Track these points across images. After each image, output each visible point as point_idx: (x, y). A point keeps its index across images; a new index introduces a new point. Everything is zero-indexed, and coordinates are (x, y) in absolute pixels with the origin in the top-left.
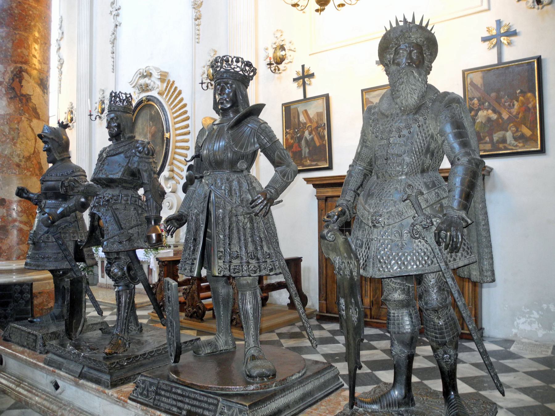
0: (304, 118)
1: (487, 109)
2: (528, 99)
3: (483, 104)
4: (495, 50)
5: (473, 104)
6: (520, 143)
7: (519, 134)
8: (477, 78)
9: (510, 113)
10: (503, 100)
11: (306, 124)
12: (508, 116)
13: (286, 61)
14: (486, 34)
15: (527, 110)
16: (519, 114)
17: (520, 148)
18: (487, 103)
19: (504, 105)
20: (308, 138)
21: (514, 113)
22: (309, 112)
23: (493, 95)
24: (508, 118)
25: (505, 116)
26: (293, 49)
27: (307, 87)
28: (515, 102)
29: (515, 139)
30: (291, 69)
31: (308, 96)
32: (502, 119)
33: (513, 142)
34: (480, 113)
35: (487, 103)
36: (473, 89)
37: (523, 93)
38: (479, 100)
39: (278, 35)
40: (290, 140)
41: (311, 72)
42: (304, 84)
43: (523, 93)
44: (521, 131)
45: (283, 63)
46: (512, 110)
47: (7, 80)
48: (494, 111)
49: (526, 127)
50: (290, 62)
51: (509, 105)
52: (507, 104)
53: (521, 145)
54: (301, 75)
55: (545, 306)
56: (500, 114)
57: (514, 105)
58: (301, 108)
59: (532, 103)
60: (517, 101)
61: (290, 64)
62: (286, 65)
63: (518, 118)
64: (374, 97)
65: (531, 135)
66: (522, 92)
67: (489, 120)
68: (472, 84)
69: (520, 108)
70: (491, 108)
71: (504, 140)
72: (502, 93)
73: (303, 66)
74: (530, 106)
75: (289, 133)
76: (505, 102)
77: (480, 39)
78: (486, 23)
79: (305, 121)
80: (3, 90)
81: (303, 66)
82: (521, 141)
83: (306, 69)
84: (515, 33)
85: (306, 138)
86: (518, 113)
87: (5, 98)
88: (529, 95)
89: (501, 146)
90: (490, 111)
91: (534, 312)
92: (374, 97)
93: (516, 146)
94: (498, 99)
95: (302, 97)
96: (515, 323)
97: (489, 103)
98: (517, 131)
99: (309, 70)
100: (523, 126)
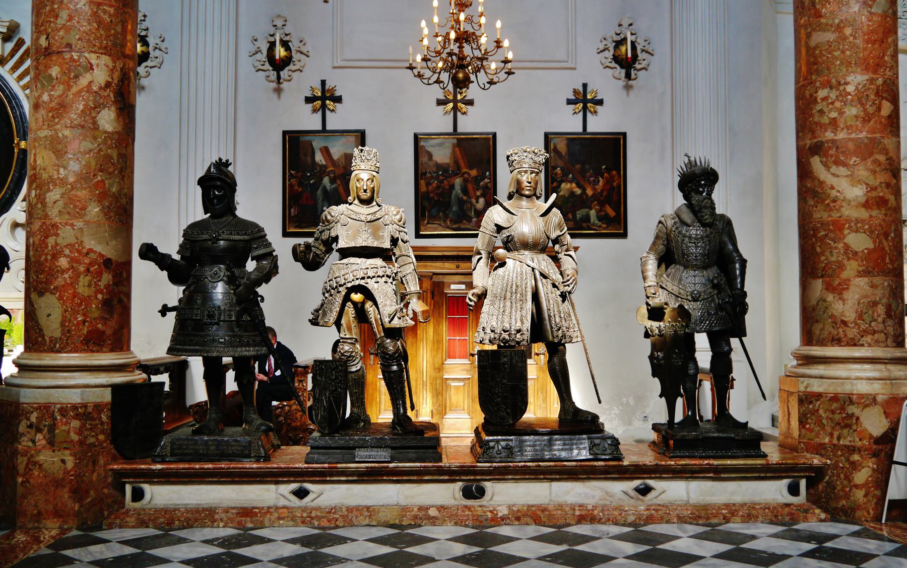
1: (571, 182)
2: (613, 177)
3: (567, 175)
5: (556, 174)
7: (603, 213)
8: (562, 146)
9: (595, 189)
11: (325, 167)
13: (291, 67)
17: (604, 229)
19: (589, 180)
20: (328, 188)
22: (332, 151)
23: (578, 166)
25: (590, 192)
26: (305, 51)
27: (328, 113)
29: (600, 219)
30: (303, 80)
31: (328, 128)
32: (587, 195)
33: (597, 222)
34: (563, 185)
37: (608, 170)
38: (562, 169)
39: (279, 23)
40: (296, 187)
41: (337, 94)
42: (324, 107)
43: (608, 170)
45: (287, 69)
47: (116, 81)
48: (579, 186)
51: (594, 181)
52: (592, 179)
53: (604, 226)
54: (320, 94)
55: (624, 400)
56: (584, 190)
57: (599, 181)
64: (433, 146)
67: (572, 193)
69: (604, 185)
71: (587, 218)
72: (587, 166)
73: (323, 83)
75: (295, 177)
77: (565, 102)
78: (569, 84)
79: (324, 163)
80: (112, 95)
81: (323, 83)
84: (600, 102)
85: (325, 187)
86: (602, 191)
87: (113, 108)
88: (614, 172)
89: (584, 225)
90: (574, 185)
92: (433, 146)
93: (600, 226)
94: (583, 172)
95: (319, 127)
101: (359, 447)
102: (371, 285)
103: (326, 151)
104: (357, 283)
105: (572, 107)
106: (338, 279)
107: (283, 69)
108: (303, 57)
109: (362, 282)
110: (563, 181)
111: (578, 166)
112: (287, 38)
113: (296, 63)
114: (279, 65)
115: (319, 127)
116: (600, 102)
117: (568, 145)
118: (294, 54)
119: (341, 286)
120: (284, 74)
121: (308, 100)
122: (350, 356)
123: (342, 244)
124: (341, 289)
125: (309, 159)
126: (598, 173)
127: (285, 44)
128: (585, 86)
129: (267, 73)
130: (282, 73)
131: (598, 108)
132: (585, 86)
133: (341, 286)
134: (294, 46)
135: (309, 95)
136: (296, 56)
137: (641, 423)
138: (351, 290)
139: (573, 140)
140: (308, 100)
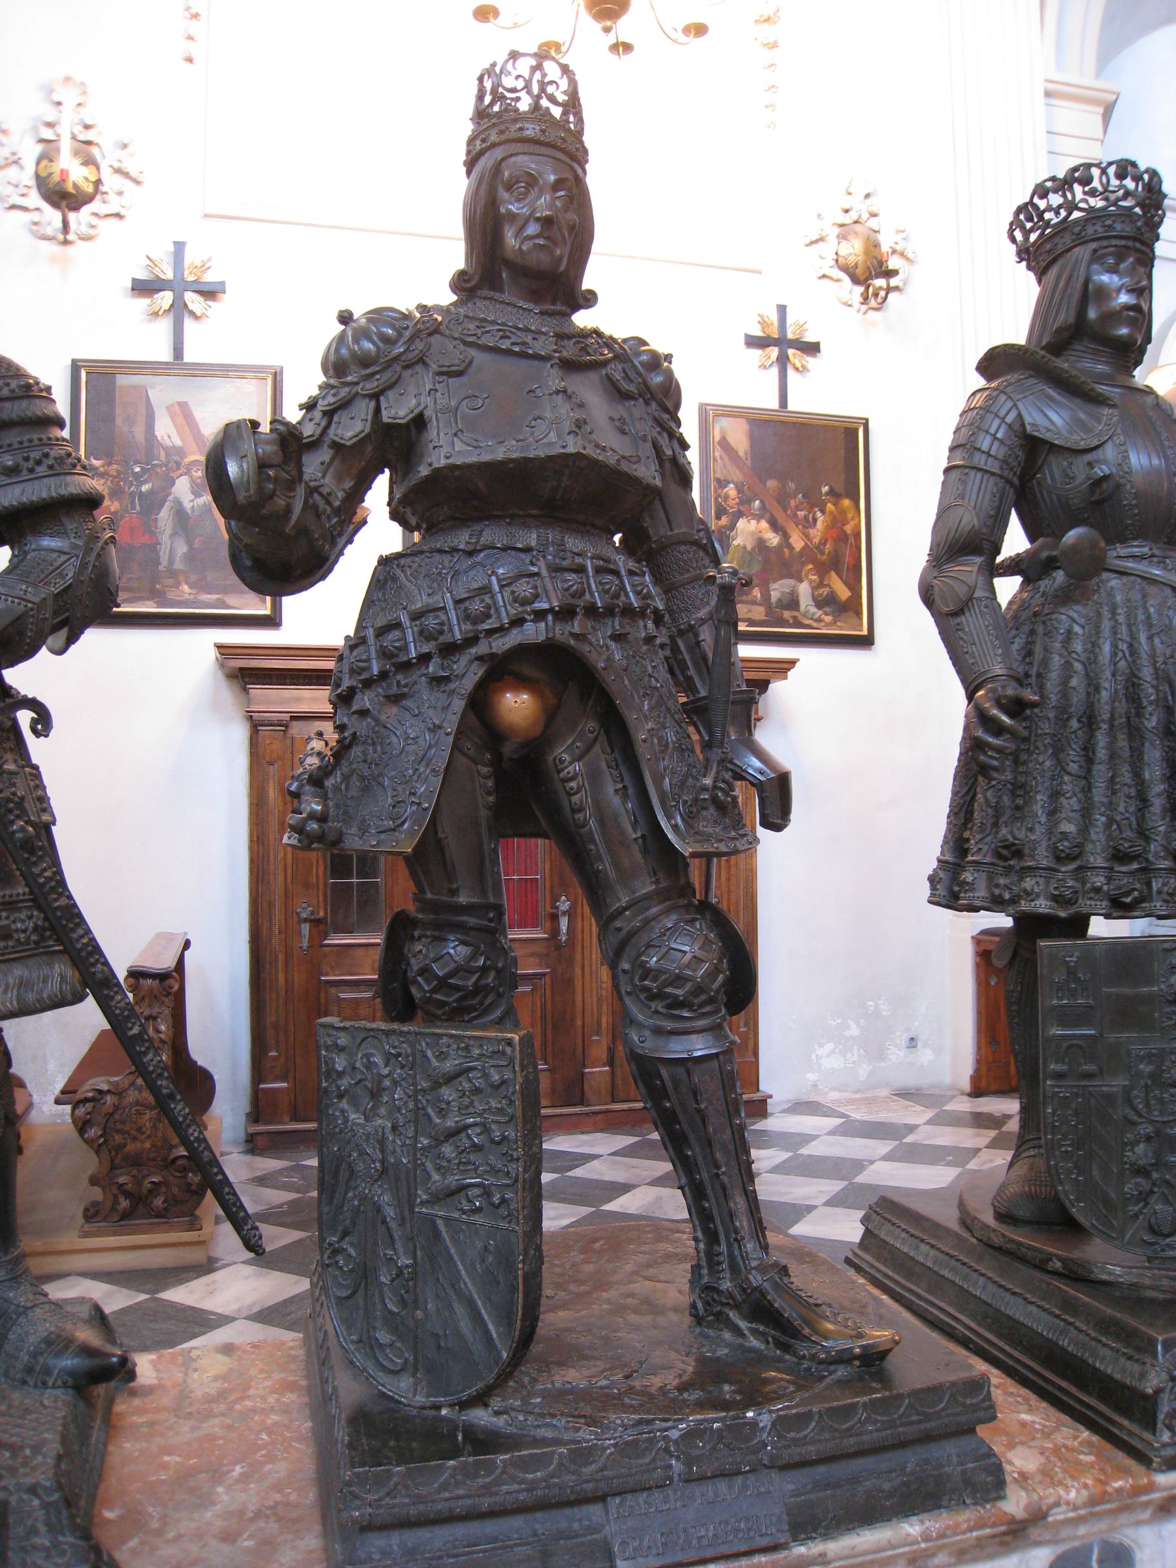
0: (173, 431)
1: (758, 518)
2: (843, 512)
3: (749, 501)
4: (775, 371)
5: (726, 497)
6: (826, 614)
7: (824, 591)
9: (807, 536)
10: (793, 503)
11: (181, 452)
12: (802, 544)
13: (95, 206)
14: (757, 332)
15: (842, 538)
16: (825, 544)
17: (828, 625)
18: (757, 502)
19: (795, 515)
20: (188, 505)
21: (816, 540)
22: (198, 414)
24: (803, 548)
25: (797, 542)
26: (133, 174)
27: (189, 324)
28: (819, 514)
29: (819, 604)
31: (189, 357)
32: (791, 548)
33: (813, 610)
34: (741, 524)
35: (757, 502)
36: (726, 458)
42: (179, 310)
44: (828, 585)
45: (86, 210)
46: (812, 532)
48: (774, 526)
49: (841, 579)
50: (118, 216)
51: (806, 518)
52: (801, 514)
53: (828, 619)
56: (786, 536)
57: (815, 520)
58: (162, 393)
59: (852, 523)
60: (823, 512)
61: (113, 221)
62: (94, 221)
63: (823, 553)
65: (849, 598)
66: (831, 492)
67: (761, 544)
68: (724, 444)
69: (828, 528)
70: (767, 515)
71: (792, 603)
73: (179, 247)
74: (848, 528)
76: (798, 508)
77: (742, 340)
79: (178, 442)
81: (179, 247)
82: (827, 609)
83: (191, 257)
85: (178, 502)
86: (823, 542)
88: (846, 502)
89: (787, 615)
90: (764, 524)
91: (851, 1022)
93: (819, 620)
94: (782, 498)
95: (162, 353)
96: (814, 1057)
97: (762, 502)
98: (821, 584)
99: (204, 268)
100: (833, 573)
101: (633, 1491)
102: (603, 650)
103: (183, 414)
104: (533, 632)
105: (757, 353)
106: (431, 622)
107: (76, 208)
108: (127, 185)
109: (561, 632)
110: (740, 514)
111: (772, 484)
112: (90, 135)
113: (112, 197)
114: (64, 198)
115: (162, 353)
116: (812, 349)
117: (751, 436)
118: (106, 175)
119: (450, 650)
120: (80, 219)
121: (144, 288)
122: (478, 989)
123: (445, 449)
124: (461, 663)
125: (139, 433)
126: (814, 502)
127: (85, 151)
128: (782, 310)
129: (35, 217)
130: (72, 216)
131: (811, 361)
132: (782, 310)
133: (450, 650)
134: (107, 156)
135: (142, 275)
136: (111, 182)
137: (902, 1053)
138: (502, 671)
139: (761, 424)
140: (144, 288)
